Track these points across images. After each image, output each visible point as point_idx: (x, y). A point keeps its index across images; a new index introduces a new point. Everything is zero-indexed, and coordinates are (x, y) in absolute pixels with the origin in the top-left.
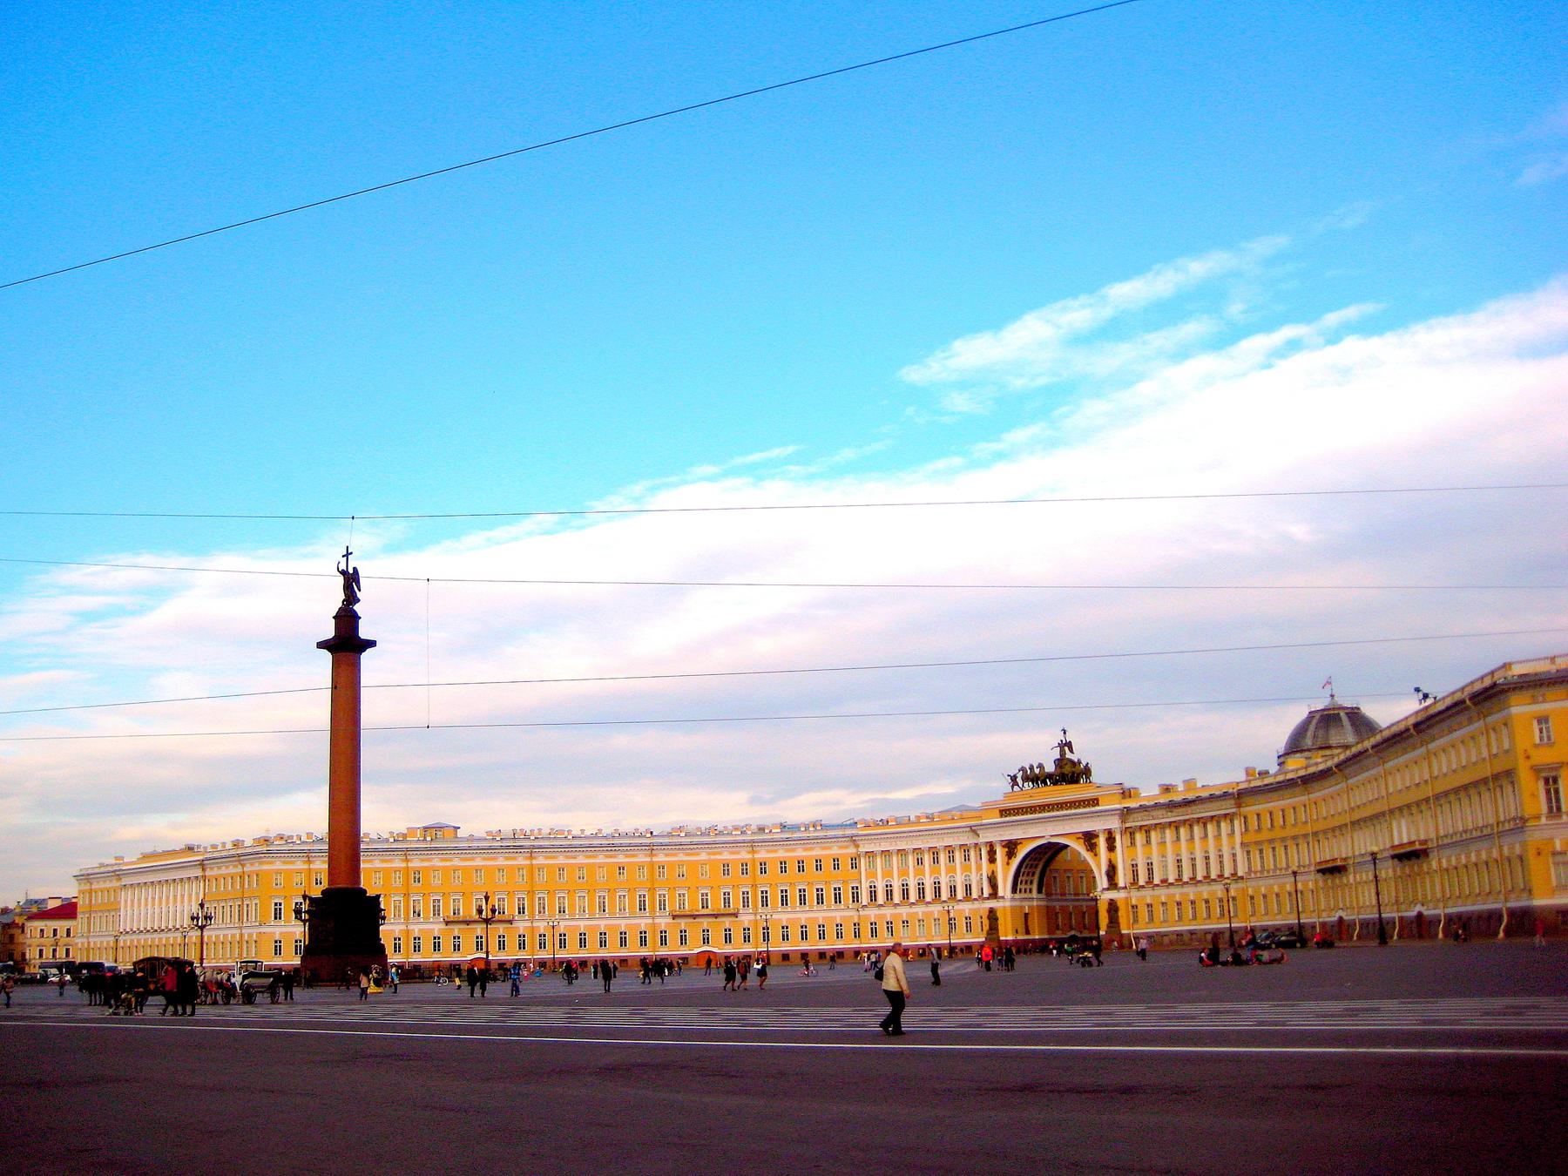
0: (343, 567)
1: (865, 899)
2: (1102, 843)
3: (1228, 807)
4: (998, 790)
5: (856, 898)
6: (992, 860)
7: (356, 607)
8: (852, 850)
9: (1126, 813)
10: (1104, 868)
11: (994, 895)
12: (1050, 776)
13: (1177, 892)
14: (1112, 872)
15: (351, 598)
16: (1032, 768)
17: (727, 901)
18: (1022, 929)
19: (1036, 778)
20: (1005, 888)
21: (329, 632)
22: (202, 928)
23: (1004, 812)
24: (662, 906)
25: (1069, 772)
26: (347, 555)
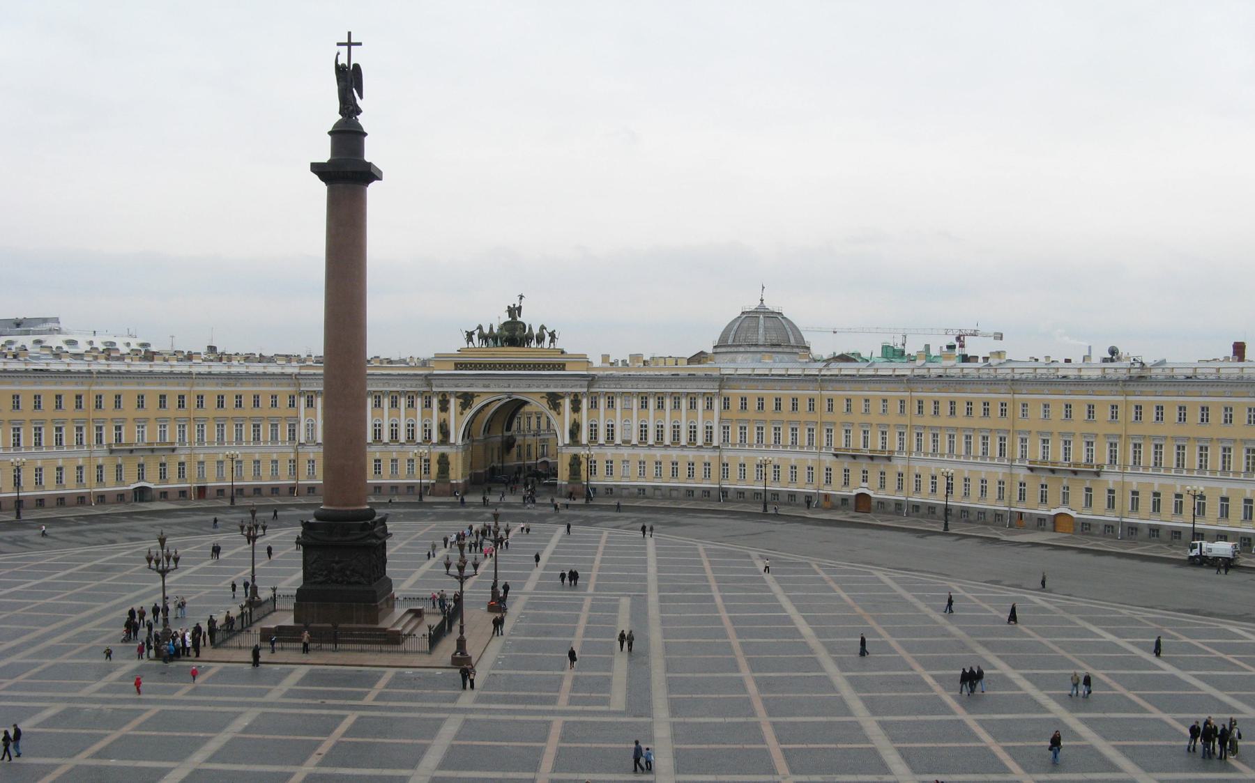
0: (343, 60)
2: (567, 404)
3: (712, 388)
4: (454, 344)
5: (292, 437)
6: (444, 407)
8: (292, 389)
9: (592, 380)
13: (642, 453)
14: (575, 430)
15: (349, 108)
16: (491, 329)
17: (163, 433)
20: (456, 436)
22: (164, 573)
23: (458, 366)
24: (99, 440)
25: (513, 333)
26: (349, 44)
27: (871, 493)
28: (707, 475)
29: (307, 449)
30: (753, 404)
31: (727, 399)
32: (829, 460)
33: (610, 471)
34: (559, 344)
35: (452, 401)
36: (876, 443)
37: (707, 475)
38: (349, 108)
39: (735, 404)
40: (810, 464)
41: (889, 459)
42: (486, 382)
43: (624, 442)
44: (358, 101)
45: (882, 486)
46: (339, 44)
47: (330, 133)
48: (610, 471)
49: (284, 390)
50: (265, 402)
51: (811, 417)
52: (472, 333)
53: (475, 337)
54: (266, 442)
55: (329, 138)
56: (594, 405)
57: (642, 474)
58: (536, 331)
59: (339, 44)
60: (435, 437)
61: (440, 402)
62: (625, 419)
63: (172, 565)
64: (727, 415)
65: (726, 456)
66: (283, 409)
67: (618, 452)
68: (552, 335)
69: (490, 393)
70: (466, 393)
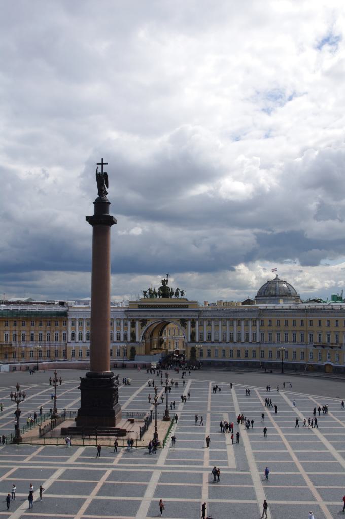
0: (100, 171)
2: (189, 324)
6: (133, 325)
10: (189, 334)
13: (224, 346)
15: (102, 192)
16: (154, 290)
19: (152, 294)
21: (91, 213)
23: (139, 307)
25: (165, 291)
26: (102, 164)
27: (332, 364)
28: (254, 356)
30: (274, 323)
31: (262, 321)
32: (311, 348)
33: (209, 355)
34: (185, 297)
35: (137, 323)
36: (333, 340)
37: (254, 356)
38: (102, 192)
39: (266, 323)
40: (302, 350)
41: (340, 347)
43: (215, 341)
44: (106, 189)
45: (338, 360)
46: (98, 164)
47: (94, 203)
48: (209, 355)
51: (302, 328)
52: (146, 292)
53: (147, 294)
54: (53, 341)
56: (201, 325)
57: (224, 356)
58: (175, 291)
59: (98, 164)
60: (129, 339)
61: (132, 323)
62: (217, 331)
63: (22, 399)
64: (262, 328)
65: (263, 347)
67: (213, 345)
68: (182, 292)
69: (153, 318)
70: (143, 319)
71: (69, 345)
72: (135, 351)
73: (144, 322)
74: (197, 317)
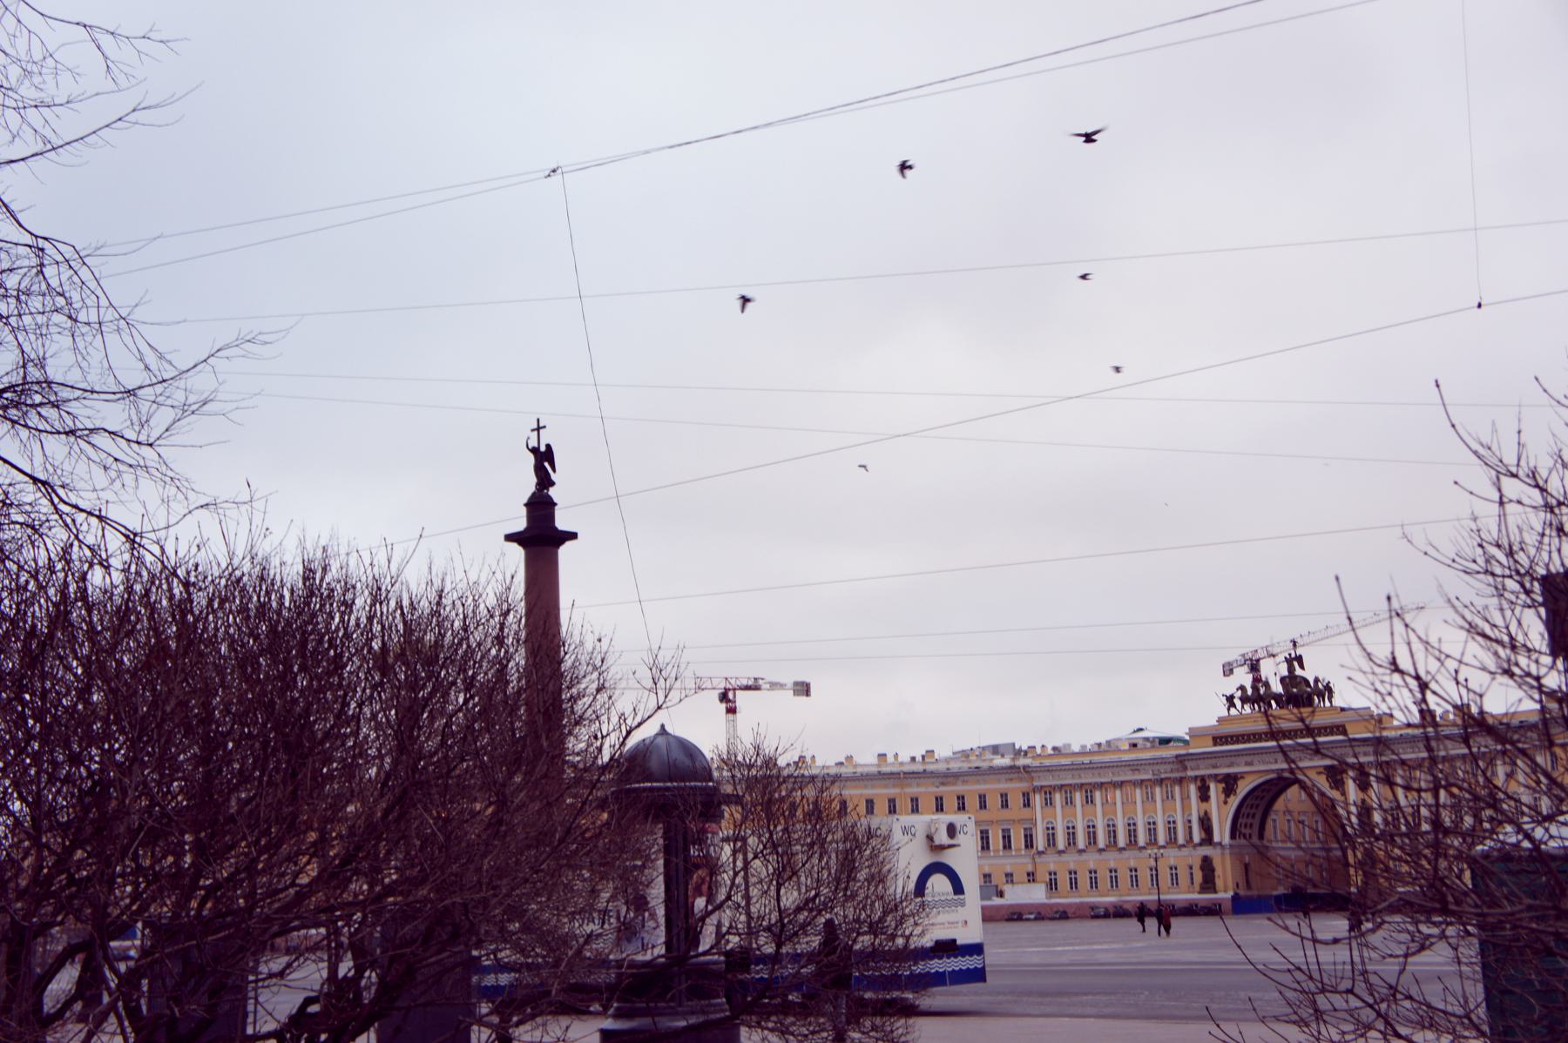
0: (533, 443)
1: (1040, 842)
5: (1029, 842)
6: (1204, 796)
7: (552, 492)
8: (1024, 786)
11: (1208, 839)
12: (1277, 697)
15: (544, 481)
18: (1242, 884)
20: (1221, 833)
21: (520, 524)
23: (1217, 740)
26: (538, 429)
29: (1044, 858)
35: (1212, 786)
38: (544, 481)
42: (1249, 759)
49: (1015, 787)
50: (994, 802)
53: (1238, 702)
55: (524, 511)
60: (1197, 836)
66: (1016, 809)
68: (1328, 688)
70: (1228, 775)
71: (1038, 860)
72: (1213, 870)
73: (1229, 783)
74: (1371, 758)
